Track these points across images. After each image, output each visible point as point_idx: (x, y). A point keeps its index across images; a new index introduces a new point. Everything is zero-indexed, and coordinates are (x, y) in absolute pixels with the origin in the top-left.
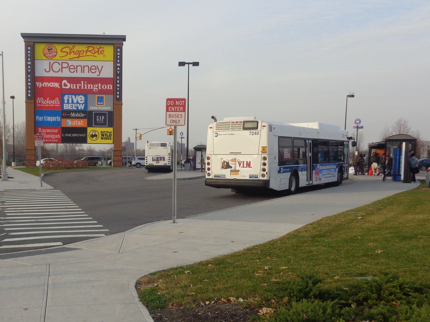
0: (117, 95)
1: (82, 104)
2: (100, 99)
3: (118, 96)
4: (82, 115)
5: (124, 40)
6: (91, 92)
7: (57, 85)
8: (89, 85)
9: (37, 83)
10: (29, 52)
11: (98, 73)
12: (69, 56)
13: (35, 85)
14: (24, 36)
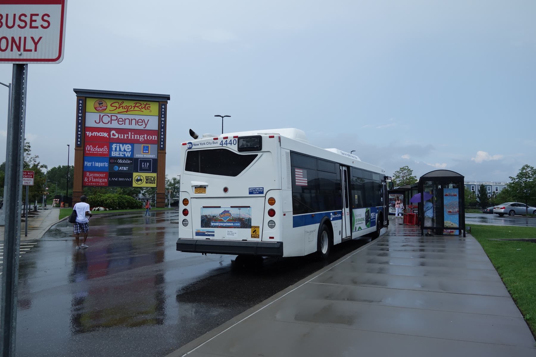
0: (161, 145)
1: (129, 152)
2: (145, 149)
3: (162, 146)
4: (129, 162)
5: (169, 99)
6: (138, 142)
7: (106, 135)
8: (136, 136)
9: (87, 133)
10: (81, 105)
11: (144, 126)
12: (118, 110)
13: (85, 134)
14: (76, 91)
